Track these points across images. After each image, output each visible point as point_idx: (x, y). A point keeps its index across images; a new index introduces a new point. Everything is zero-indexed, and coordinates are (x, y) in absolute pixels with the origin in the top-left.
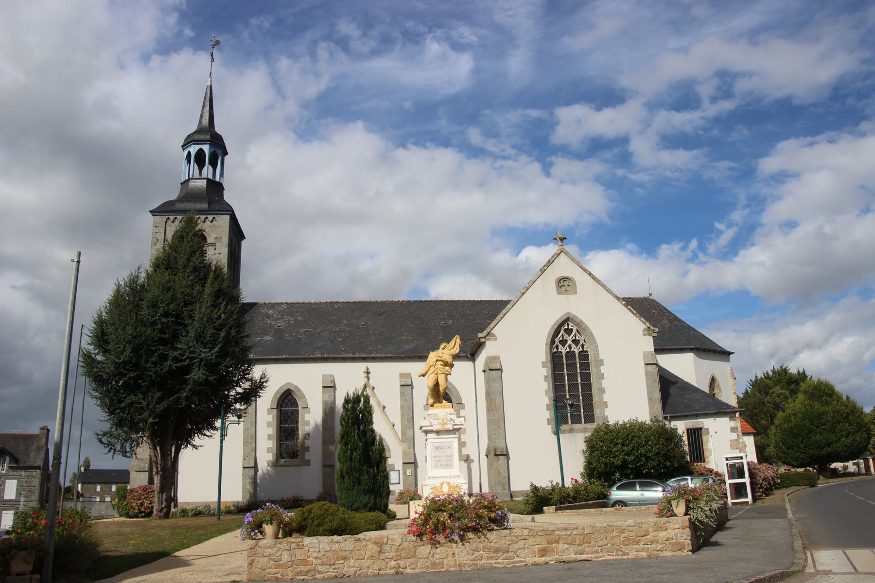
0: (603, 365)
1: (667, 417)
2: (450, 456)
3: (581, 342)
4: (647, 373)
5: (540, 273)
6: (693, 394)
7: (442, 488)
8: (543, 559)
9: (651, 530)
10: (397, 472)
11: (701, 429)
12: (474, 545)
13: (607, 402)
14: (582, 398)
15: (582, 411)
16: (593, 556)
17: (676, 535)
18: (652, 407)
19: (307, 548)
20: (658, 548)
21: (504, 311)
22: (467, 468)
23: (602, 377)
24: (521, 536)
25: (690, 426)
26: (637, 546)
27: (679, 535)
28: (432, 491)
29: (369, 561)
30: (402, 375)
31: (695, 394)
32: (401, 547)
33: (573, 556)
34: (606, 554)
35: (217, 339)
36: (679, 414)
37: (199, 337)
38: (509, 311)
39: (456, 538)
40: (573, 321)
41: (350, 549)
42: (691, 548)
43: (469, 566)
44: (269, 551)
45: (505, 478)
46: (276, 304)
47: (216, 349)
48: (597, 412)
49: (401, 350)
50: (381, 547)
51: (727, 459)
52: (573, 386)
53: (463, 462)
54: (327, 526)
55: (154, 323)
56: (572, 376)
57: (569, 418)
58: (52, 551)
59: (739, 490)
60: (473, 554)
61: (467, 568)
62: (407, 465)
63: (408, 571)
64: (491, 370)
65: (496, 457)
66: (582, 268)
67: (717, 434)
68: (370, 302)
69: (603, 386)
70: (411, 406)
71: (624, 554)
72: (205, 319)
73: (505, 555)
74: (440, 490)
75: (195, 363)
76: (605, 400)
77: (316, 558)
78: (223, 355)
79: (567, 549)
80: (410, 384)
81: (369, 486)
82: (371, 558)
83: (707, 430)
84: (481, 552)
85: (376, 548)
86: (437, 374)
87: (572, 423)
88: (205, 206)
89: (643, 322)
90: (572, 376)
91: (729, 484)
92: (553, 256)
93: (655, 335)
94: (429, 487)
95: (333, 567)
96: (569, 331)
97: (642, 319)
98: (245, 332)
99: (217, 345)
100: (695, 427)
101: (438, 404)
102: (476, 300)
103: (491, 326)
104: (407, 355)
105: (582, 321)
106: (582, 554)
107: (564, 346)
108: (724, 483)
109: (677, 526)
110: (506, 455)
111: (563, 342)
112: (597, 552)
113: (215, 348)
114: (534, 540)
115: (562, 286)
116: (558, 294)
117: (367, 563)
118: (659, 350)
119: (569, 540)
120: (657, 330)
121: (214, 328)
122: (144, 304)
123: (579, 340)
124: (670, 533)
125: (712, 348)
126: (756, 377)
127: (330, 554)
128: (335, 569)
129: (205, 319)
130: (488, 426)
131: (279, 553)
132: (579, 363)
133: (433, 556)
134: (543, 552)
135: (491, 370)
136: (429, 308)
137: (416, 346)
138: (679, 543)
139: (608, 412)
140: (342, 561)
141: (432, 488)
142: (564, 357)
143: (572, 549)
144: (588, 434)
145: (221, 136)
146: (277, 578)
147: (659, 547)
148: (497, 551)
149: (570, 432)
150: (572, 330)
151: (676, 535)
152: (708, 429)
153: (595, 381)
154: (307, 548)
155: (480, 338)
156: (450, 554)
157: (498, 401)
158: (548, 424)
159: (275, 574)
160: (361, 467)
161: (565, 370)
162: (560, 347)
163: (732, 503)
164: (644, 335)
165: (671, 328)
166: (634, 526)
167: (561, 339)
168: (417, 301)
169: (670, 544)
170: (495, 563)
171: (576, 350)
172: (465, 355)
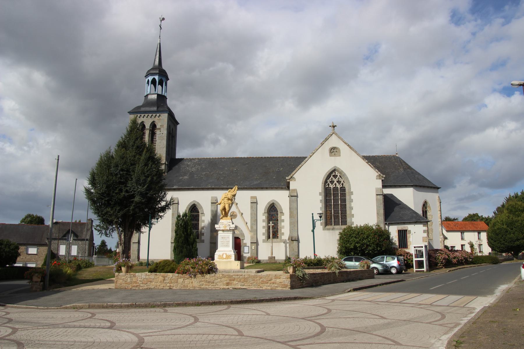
0: (353, 194)
1: (387, 223)
2: (228, 242)
3: (342, 182)
4: (377, 199)
5: (321, 145)
6: (406, 211)
7: (223, 256)
8: (227, 287)
9: (273, 278)
10: (248, 247)
11: (406, 230)
12: (200, 279)
13: (353, 214)
14: (341, 212)
15: (340, 219)
16: (248, 287)
17: (284, 281)
18: (378, 217)
19: (137, 277)
20: (276, 286)
21: (300, 166)
22: (285, 246)
23: (352, 201)
24: (219, 277)
25: (400, 229)
26: (267, 285)
27: (285, 281)
28: (218, 257)
29: (160, 283)
30: (252, 197)
31: (407, 211)
32: (172, 278)
33: (239, 287)
34: (253, 287)
35: (146, 182)
36: (393, 222)
37: (138, 182)
38: (303, 165)
39: (193, 276)
40: (338, 171)
41: (153, 278)
42: (290, 287)
43: (198, 288)
44: (123, 277)
45: (296, 252)
46: (193, 159)
47: (146, 187)
48: (348, 220)
49: (252, 184)
50: (164, 278)
51: (415, 247)
52: (336, 205)
53: (283, 243)
54: (165, 270)
55: (116, 175)
56: (336, 201)
57: (333, 223)
58: (48, 274)
59: (420, 264)
60: (200, 283)
61: (197, 288)
62: (252, 244)
63: (174, 288)
64: (291, 196)
65: (292, 241)
66: (344, 142)
67: (415, 233)
68: (241, 158)
69: (352, 206)
70: (256, 213)
71: (261, 287)
72: (140, 172)
73: (212, 284)
74: (222, 257)
75: (136, 193)
76: (353, 213)
77: (140, 281)
78: (149, 189)
79: (237, 283)
80: (256, 202)
81: (186, 254)
82: (161, 282)
83: (410, 231)
84: (203, 282)
85: (163, 278)
86: (225, 204)
87: (334, 225)
88: (155, 109)
89: (376, 172)
90: (336, 201)
91: (415, 260)
92: (329, 136)
93: (383, 179)
94: (217, 255)
95: (147, 285)
96: (335, 176)
97: (376, 170)
98: (163, 177)
99: (146, 185)
100: (403, 229)
101: (225, 218)
102: (298, 156)
103: (293, 173)
104: (254, 187)
105: (342, 171)
106: (243, 286)
107: (332, 184)
108: (412, 261)
109: (285, 277)
110: (298, 240)
111: (332, 182)
112: (249, 286)
113: (145, 186)
114: (224, 279)
115: (333, 152)
116: (330, 156)
117: (158, 284)
118: (384, 186)
119: (238, 280)
120: (384, 176)
121: (145, 176)
122: (112, 165)
123: (341, 181)
124: (281, 280)
125: (427, 185)
126: (510, 196)
127: (145, 280)
128: (147, 285)
129: (140, 172)
130: (290, 225)
131: (127, 278)
132: (340, 193)
133: (184, 283)
134: (228, 284)
135: (291, 196)
136: (272, 161)
137: (261, 182)
138: (285, 285)
139: (353, 220)
140: (150, 283)
141: (219, 256)
142: (332, 190)
143: (240, 284)
144: (341, 231)
145: (165, 70)
146: (125, 288)
147: (276, 285)
148: (209, 282)
149: (333, 230)
150: (337, 175)
151: (284, 281)
152: (410, 230)
153: (348, 203)
154: (137, 277)
155: (287, 180)
156: (191, 282)
157: (295, 212)
158: (321, 225)
159: (125, 286)
160: (183, 245)
161: (332, 197)
162: (330, 184)
163: (416, 271)
164: (377, 179)
165: (404, 173)
166: (266, 276)
167: (331, 180)
168: (266, 157)
169: (281, 284)
170: (208, 287)
171: (339, 186)
172: (285, 187)
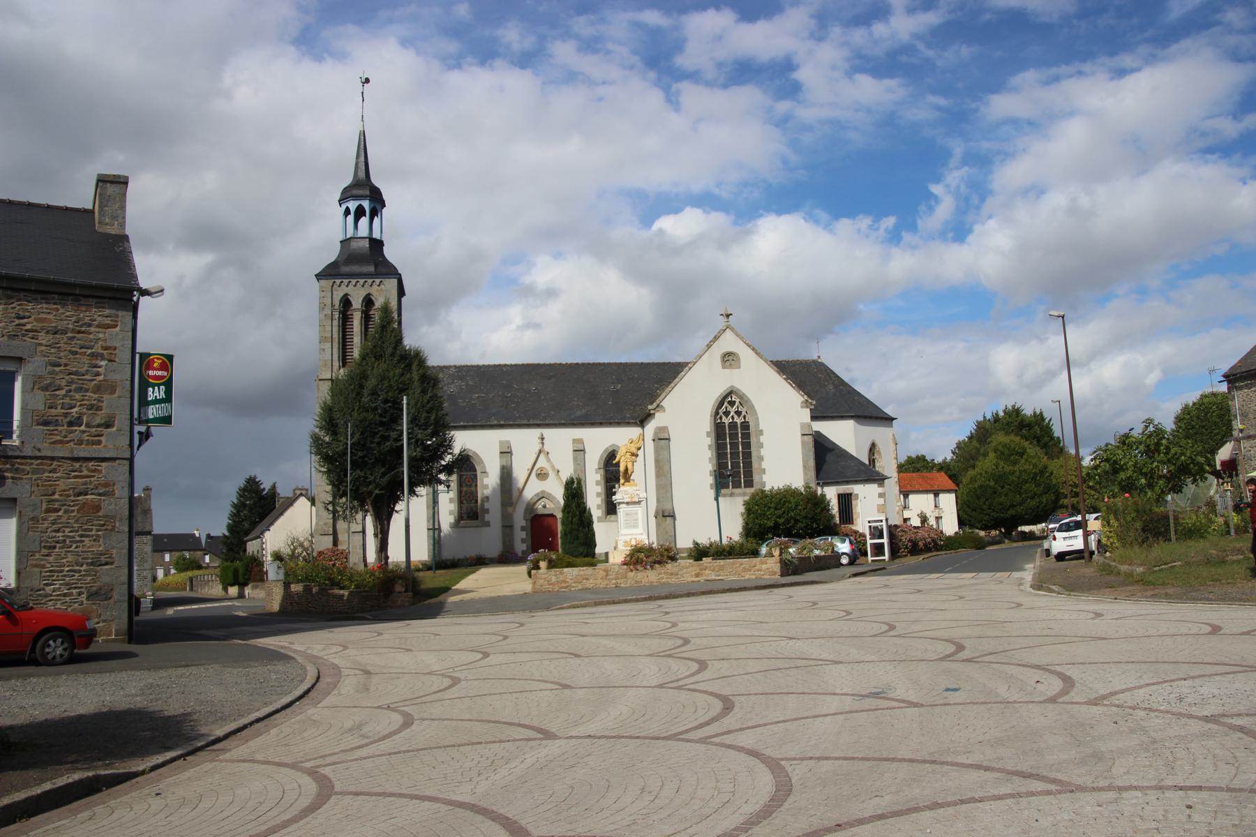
0: (762, 435)
3: (744, 413)
4: (803, 443)
8: (697, 579)
9: (758, 563)
15: (742, 476)
23: (761, 446)
25: (841, 492)
30: (575, 441)
33: (714, 577)
39: (648, 567)
40: (736, 394)
42: (780, 574)
44: (544, 576)
45: (671, 536)
46: (444, 367)
48: (756, 478)
49: (573, 417)
51: (869, 522)
52: (735, 454)
55: (376, 409)
56: (734, 445)
59: (878, 549)
63: (622, 585)
68: (539, 364)
73: (676, 576)
76: (763, 467)
77: (571, 579)
83: (857, 495)
85: (605, 574)
87: (733, 487)
88: (371, 269)
89: (801, 395)
90: (734, 445)
92: (719, 332)
93: (813, 407)
94: (621, 542)
96: (732, 403)
97: (801, 392)
103: (661, 398)
105: (744, 394)
107: (727, 417)
108: (865, 544)
110: (673, 516)
111: (727, 413)
112: (727, 575)
122: (366, 392)
123: (741, 412)
125: (875, 414)
126: (984, 417)
134: (697, 575)
139: (765, 478)
142: (727, 428)
144: (747, 498)
145: (379, 189)
146: (549, 591)
147: (762, 573)
148: (671, 574)
150: (735, 401)
153: (755, 449)
161: (728, 440)
163: (872, 561)
164: (802, 407)
167: (725, 410)
171: (738, 420)
172: (634, 421)
